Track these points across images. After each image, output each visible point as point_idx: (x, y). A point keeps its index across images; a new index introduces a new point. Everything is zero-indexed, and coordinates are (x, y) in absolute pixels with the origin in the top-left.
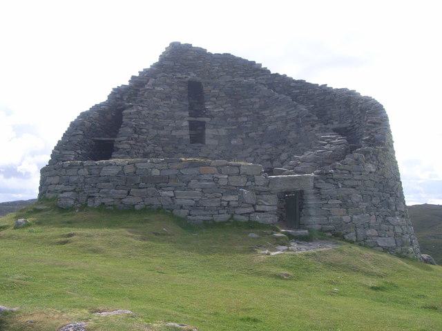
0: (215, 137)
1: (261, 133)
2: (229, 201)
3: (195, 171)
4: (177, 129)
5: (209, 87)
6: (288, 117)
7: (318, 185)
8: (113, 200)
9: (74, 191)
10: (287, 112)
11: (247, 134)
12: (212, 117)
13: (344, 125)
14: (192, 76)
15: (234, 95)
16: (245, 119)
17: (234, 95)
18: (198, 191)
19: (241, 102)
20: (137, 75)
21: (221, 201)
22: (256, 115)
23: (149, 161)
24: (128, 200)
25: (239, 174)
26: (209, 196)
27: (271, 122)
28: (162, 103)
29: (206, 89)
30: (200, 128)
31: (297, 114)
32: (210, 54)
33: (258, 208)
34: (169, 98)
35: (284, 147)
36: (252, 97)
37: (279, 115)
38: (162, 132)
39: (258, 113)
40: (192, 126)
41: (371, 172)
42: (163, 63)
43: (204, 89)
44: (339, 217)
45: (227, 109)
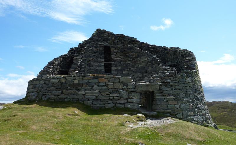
0: (115, 70)
1: (136, 68)
2: (114, 97)
3: (96, 81)
4: (99, 66)
5: (113, 49)
6: (148, 61)
7: (162, 88)
8: (54, 96)
9: (37, 92)
10: (148, 59)
11: (130, 69)
12: (114, 61)
13: (174, 64)
14: (106, 44)
15: (124, 52)
16: (129, 62)
17: (124, 52)
18: (97, 91)
19: (127, 55)
20: (82, 43)
21: (110, 96)
22: (133, 61)
23: (73, 76)
24: (62, 96)
25: (119, 82)
26: (103, 94)
27: (140, 63)
28: (92, 55)
29: (112, 49)
30: (110, 67)
31: (152, 59)
32: (114, 34)
33: (129, 100)
34: (95, 53)
35: (146, 74)
36: (132, 53)
37: (143, 60)
38: (92, 68)
39: (135, 60)
40: (106, 66)
41: (189, 82)
42: (94, 38)
43: (111, 49)
44: (173, 105)
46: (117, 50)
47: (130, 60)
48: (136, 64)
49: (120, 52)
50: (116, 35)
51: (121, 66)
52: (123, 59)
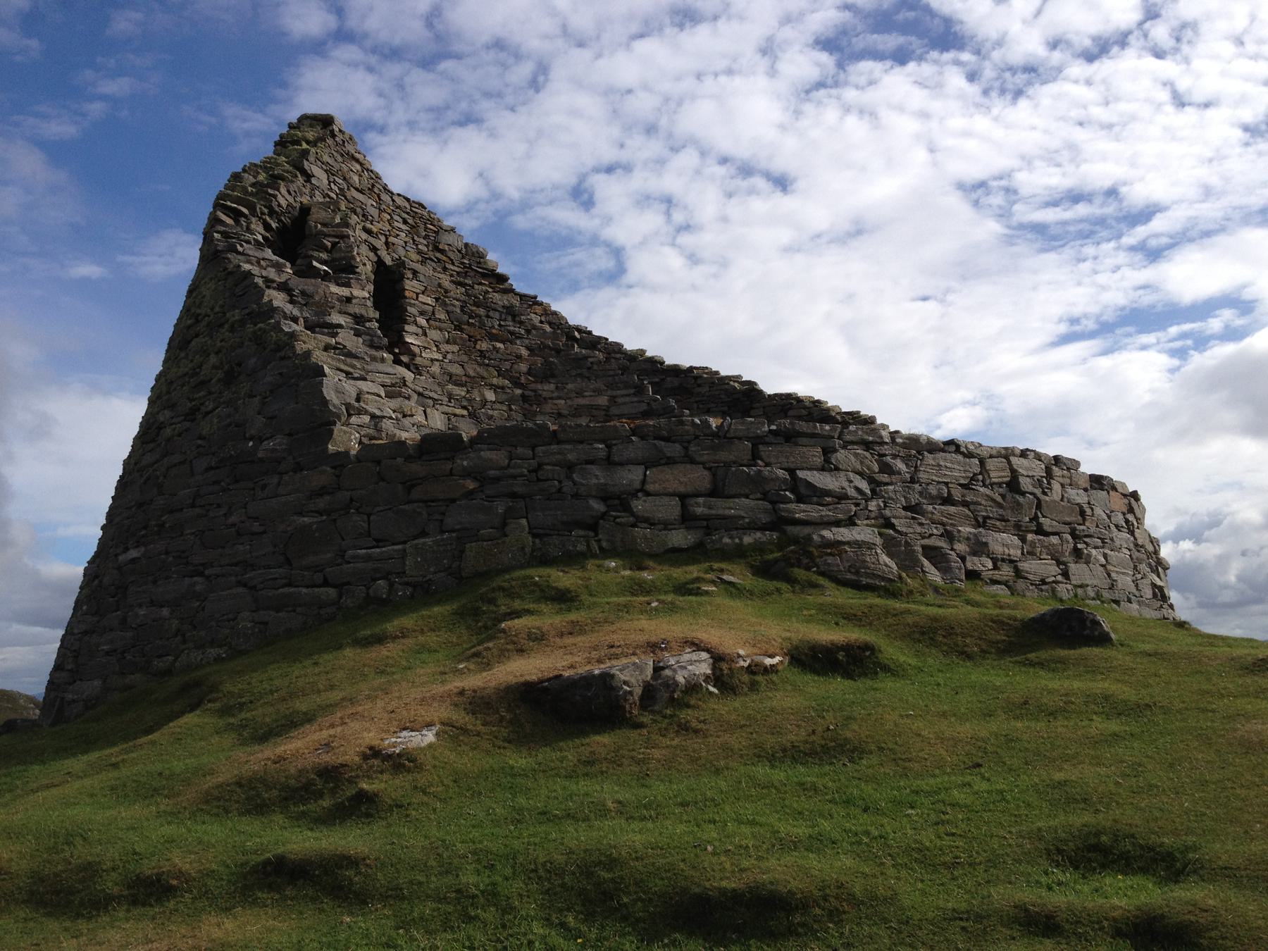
10: (613, 399)
17: (469, 324)
22: (518, 392)
29: (411, 286)
37: (582, 401)
45: (449, 356)
46: (429, 301)
47: (495, 381)
48: (535, 414)
49: (443, 316)
50: (399, 201)
51: (450, 410)
52: (456, 369)
